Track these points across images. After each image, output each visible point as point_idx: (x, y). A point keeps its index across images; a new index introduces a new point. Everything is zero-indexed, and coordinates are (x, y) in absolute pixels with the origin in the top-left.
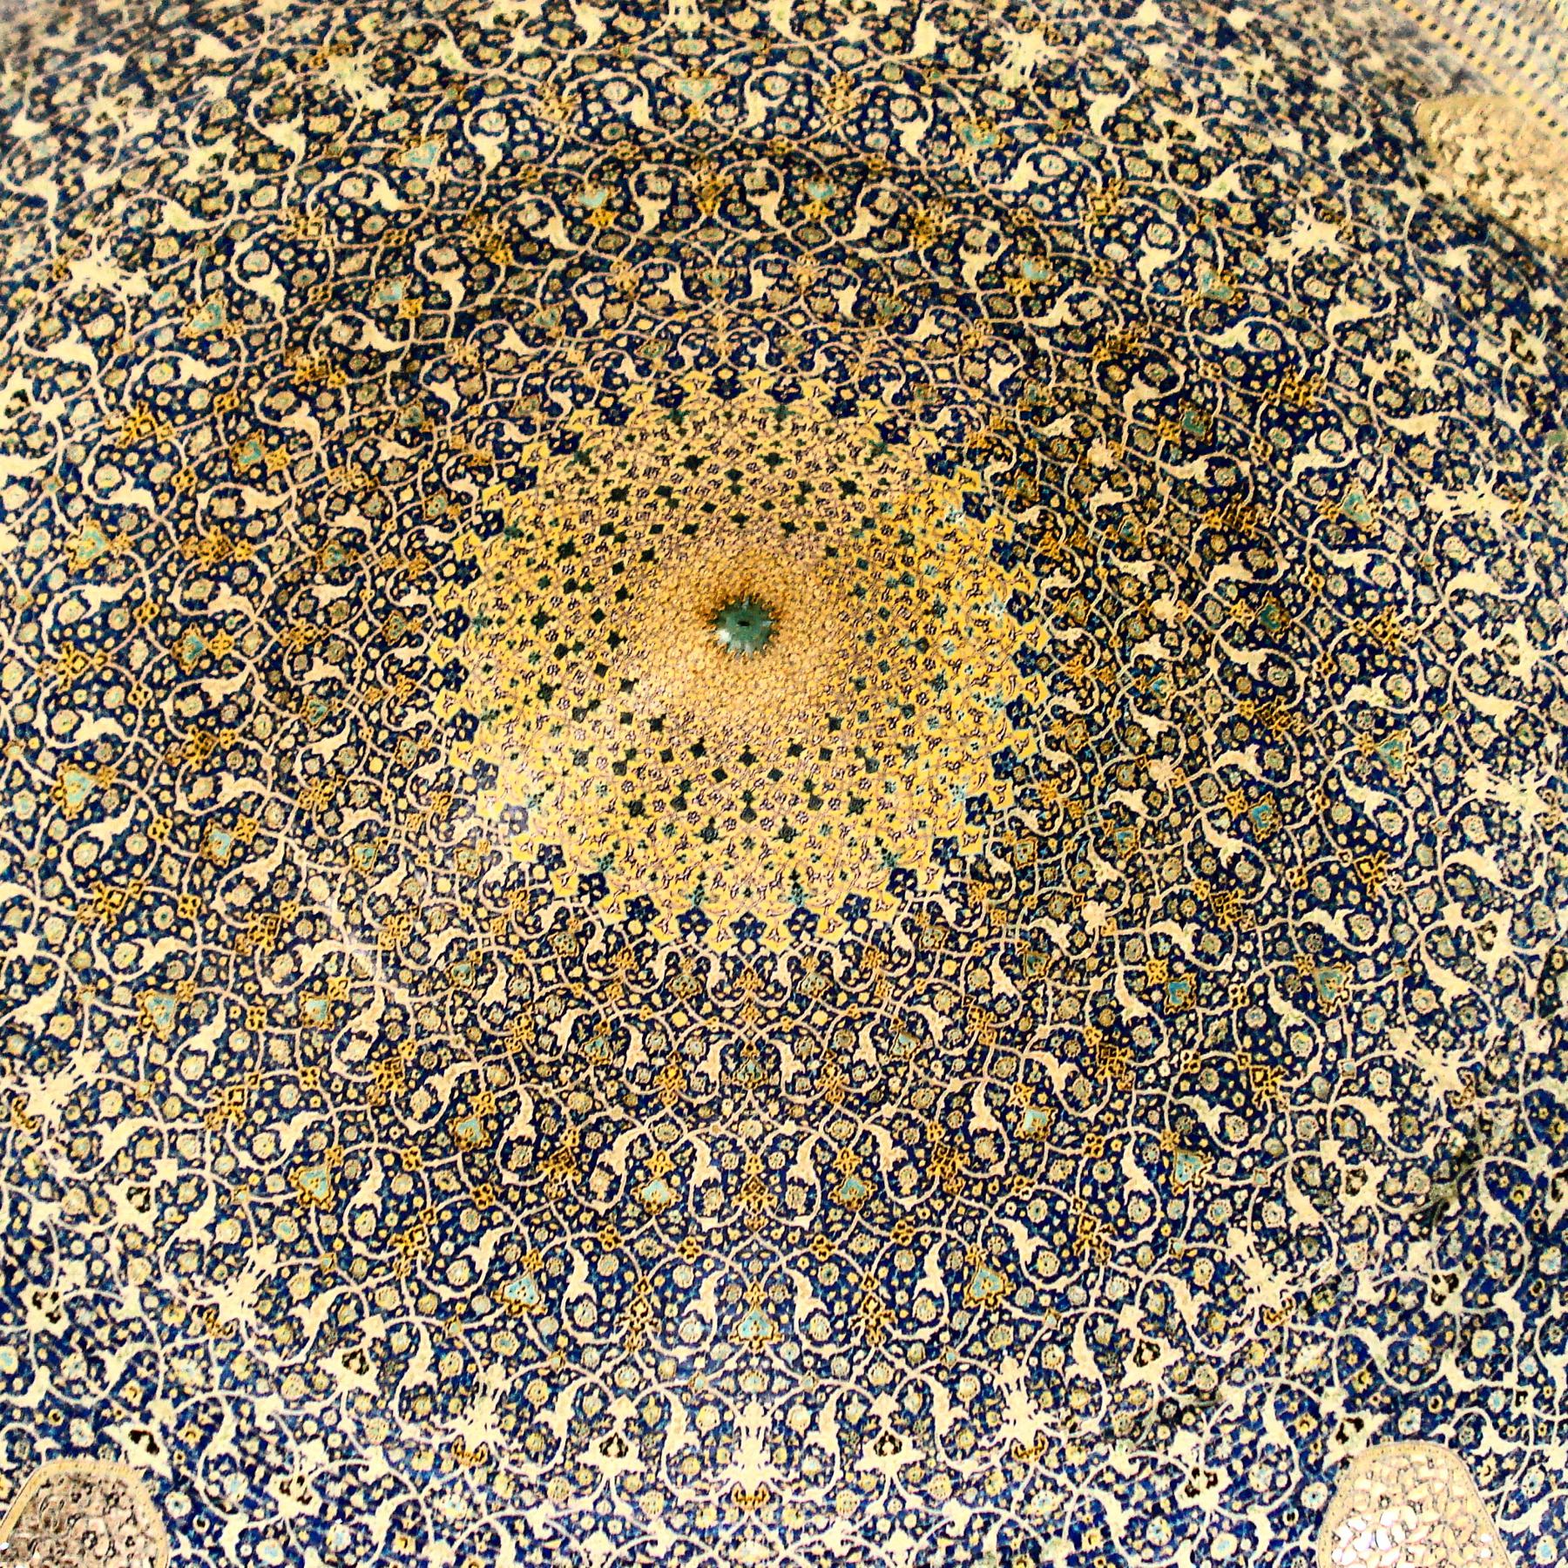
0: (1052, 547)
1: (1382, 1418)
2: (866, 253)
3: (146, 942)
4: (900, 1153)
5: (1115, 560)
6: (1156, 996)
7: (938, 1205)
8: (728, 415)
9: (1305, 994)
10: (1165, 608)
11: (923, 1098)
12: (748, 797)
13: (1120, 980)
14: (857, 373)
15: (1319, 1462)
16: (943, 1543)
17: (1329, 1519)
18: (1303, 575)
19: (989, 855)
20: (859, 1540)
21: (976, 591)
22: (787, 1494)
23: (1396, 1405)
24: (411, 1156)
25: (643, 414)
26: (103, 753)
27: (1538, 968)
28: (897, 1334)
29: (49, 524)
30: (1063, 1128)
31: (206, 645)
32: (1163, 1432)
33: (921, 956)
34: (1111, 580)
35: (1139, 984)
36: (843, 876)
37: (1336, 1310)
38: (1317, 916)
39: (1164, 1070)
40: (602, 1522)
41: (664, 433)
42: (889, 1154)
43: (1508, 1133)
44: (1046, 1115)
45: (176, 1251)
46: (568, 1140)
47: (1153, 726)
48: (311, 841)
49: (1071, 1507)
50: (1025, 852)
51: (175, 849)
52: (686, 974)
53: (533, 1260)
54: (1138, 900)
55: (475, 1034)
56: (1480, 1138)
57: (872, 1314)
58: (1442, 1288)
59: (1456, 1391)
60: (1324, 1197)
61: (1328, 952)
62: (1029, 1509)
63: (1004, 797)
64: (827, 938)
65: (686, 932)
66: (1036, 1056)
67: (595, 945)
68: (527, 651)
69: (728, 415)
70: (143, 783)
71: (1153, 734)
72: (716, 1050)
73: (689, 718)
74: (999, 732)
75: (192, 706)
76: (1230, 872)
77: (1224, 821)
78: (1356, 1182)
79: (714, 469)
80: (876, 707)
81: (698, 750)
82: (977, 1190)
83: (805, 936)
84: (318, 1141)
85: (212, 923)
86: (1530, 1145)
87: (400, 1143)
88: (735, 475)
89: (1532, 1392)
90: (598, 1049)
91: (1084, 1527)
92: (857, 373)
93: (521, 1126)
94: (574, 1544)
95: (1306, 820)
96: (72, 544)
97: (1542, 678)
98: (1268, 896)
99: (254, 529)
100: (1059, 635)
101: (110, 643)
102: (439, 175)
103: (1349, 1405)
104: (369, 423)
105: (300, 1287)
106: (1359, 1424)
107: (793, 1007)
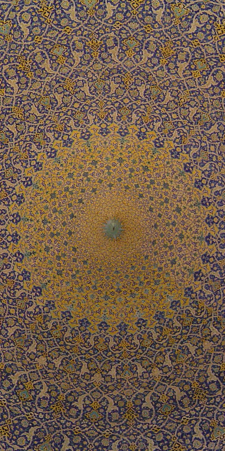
0: (167, 331)
5: (168, 353)
6: (21, 387)
8: (199, 221)
9: (38, 440)
10: (156, 372)
12: (58, 234)
18: (186, 418)
19: (53, 321)
21: (143, 307)
25: (198, 193)
26: (100, 12)
34: (161, 353)
35: (23, 380)
36: (36, 270)
38: (67, 440)
41: (191, 200)
47: (113, 372)
48: (54, 82)
50: (56, 333)
51: (60, 35)
54: (51, 375)
63: (73, 324)
64: (15, 266)
68: (137, 160)
69: (199, 221)
70: (86, 25)
71: (109, 373)
73: (83, 212)
74: (95, 321)
75: (110, 43)
76: (71, 407)
77: (88, 402)
81: (72, 216)
83: (15, 258)
85: (31, 48)
88: (174, 224)
95: (98, 430)
96: (181, 6)
98: (67, 421)
99: (171, 66)
100: (135, 337)
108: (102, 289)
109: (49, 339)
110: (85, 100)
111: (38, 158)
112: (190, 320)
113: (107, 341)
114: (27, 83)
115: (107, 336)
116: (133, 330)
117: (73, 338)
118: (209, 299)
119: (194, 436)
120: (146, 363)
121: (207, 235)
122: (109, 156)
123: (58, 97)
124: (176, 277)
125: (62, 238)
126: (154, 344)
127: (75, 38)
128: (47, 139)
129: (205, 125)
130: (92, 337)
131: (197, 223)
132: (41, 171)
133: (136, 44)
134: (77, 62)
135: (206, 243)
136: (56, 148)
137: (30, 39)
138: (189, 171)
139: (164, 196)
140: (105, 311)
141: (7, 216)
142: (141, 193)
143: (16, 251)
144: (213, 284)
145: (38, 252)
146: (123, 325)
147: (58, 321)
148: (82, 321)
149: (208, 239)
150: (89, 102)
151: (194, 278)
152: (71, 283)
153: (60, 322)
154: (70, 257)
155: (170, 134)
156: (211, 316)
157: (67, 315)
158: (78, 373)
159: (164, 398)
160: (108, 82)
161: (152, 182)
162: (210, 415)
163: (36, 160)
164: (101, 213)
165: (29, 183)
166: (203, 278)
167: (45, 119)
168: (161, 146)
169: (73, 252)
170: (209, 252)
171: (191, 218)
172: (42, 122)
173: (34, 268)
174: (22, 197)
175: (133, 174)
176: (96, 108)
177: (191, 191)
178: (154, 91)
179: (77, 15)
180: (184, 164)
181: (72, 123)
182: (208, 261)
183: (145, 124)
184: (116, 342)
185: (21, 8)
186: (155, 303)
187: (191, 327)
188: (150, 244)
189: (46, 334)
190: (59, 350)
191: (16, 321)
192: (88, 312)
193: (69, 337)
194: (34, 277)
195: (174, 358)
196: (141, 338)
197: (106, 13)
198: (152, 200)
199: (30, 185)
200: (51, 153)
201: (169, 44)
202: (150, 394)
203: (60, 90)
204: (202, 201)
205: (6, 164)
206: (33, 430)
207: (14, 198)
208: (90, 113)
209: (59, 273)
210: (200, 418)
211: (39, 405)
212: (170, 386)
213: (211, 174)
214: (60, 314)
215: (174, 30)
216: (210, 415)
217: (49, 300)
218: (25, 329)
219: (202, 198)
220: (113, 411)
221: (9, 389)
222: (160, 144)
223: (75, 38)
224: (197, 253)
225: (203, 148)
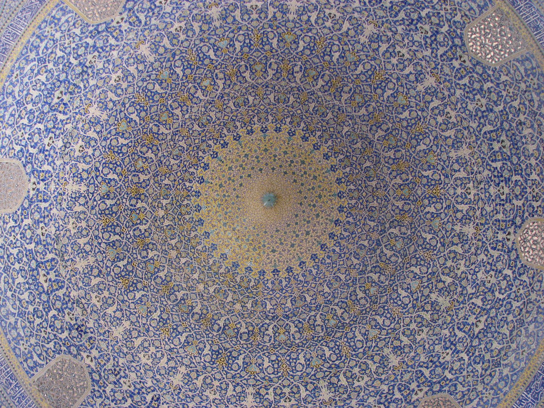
0: (229, 276)
1: (31, 196)
2: (313, 313)
3: (364, 71)
4: (160, 132)
5: (217, 286)
6: (138, 212)
7: (145, 130)
9: (114, 245)
10: (201, 287)
11: (164, 146)
12: (244, 169)
13: (146, 207)
14: (293, 281)
15: (33, 174)
16: (91, 74)
17: (22, 168)
18: (187, 323)
19: (189, 202)
20: (109, 58)
22: (132, 52)
23: (31, 202)
24: (269, 54)
26: (400, 110)
27: (86, 306)
28: (133, 100)
29: (444, 162)
30: (133, 169)
31: (389, 142)
32: (66, 141)
34: (214, 281)
35: (142, 210)
36: (213, 171)
37: (56, 200)
38: (125, 262)
39: (124, 200)
40: (171, 14)
42: (163, 130)
43: (61, 272)
44: (138, 167)
45: (316, 8)
46: (234, 79)
47: (183, 260)
48: (337, 107)
49: (71, 108)
52: (231, 127)
53: (225, 51)
54: (156, 224)
55: (270, 86)
56: (64, 264)
57: (141, 98)
58: (44, 231)
59: (25, 220)
60: (77, 215)
61: (118, 257)
62: (79, 98)
63: (195, 216)
66: (149, 176)
67: (256, 119)
69: (309, 250)
70: (386, 106)
71: (181, 259)
72: (214, 118)
73: (267, 175)
75: (384, 127)
76: (146, 250)
77: (156, 258)
78: (74, 225)
80: (232, 208)
82: (139, 141)
83: (212, 153)
84: (294, 46)
85: (350, 80)
86: (56, 276)
87: (274, 56)
88: (297, 236)
89: (14, 241)
90: (241, 100)
91: (65, 108)
92: (293, 281)
93: (247, 75)
94: (175, 5)
96: (435, 158)
97: (138, 359)
99: (394, 173)
100: (213, 259)
101: (413, 136)
102: (408, 281)
103: (38, 189)
104: (384, 209)
105: (279, 15)
106: (34, 189)
107: (204, 138)
110: (339, 133)
111: (284, 127)
113: (199, 243)
114: (326, 91)
119: (179, 336)
120: (202, 277)
122: (313, 169)
123: (330, 115)
125: (243, 173)
126: (217, 274)
127: (374, 104)
128: (299, 125)
129: (371, 217)
133: (394, 143)
134: (359, 114)
136: (297, 134)
137: (355, 76)
138: (336, 224)
143: (217, 150)
144: (277, 284)
148: (201, 220)
150: (339, 136)
155: (351, 198)
157: (198, 208)
158: (169, 239)
159: (189, 302)
160: (359, 140)
161: (314, 206)
162: (198, 337)
168: (340, 197)
172: (308, 115)
174: (252, 133)
178: (372, 173)
179: (388, 97)
181: (319, 133)
182: (288, 272)
185: (371, 60)
190: (174, 218)
191: (175, 180)
194: (208, 172)
195: (216, 291)
197: (401, 113)
201: (406, 164)
202: (186, 292)
203: (335, 114)
206: (117, 237)
209: (221, 186)
210: (193, 332)
211: (134, 230)
212: (199, 301)
214: (196, 203)
215: (417, 162)
216: (198, 337)
220: (161, 277)
221: (132, 205)
223: (374, 104)
225: (356, 224)
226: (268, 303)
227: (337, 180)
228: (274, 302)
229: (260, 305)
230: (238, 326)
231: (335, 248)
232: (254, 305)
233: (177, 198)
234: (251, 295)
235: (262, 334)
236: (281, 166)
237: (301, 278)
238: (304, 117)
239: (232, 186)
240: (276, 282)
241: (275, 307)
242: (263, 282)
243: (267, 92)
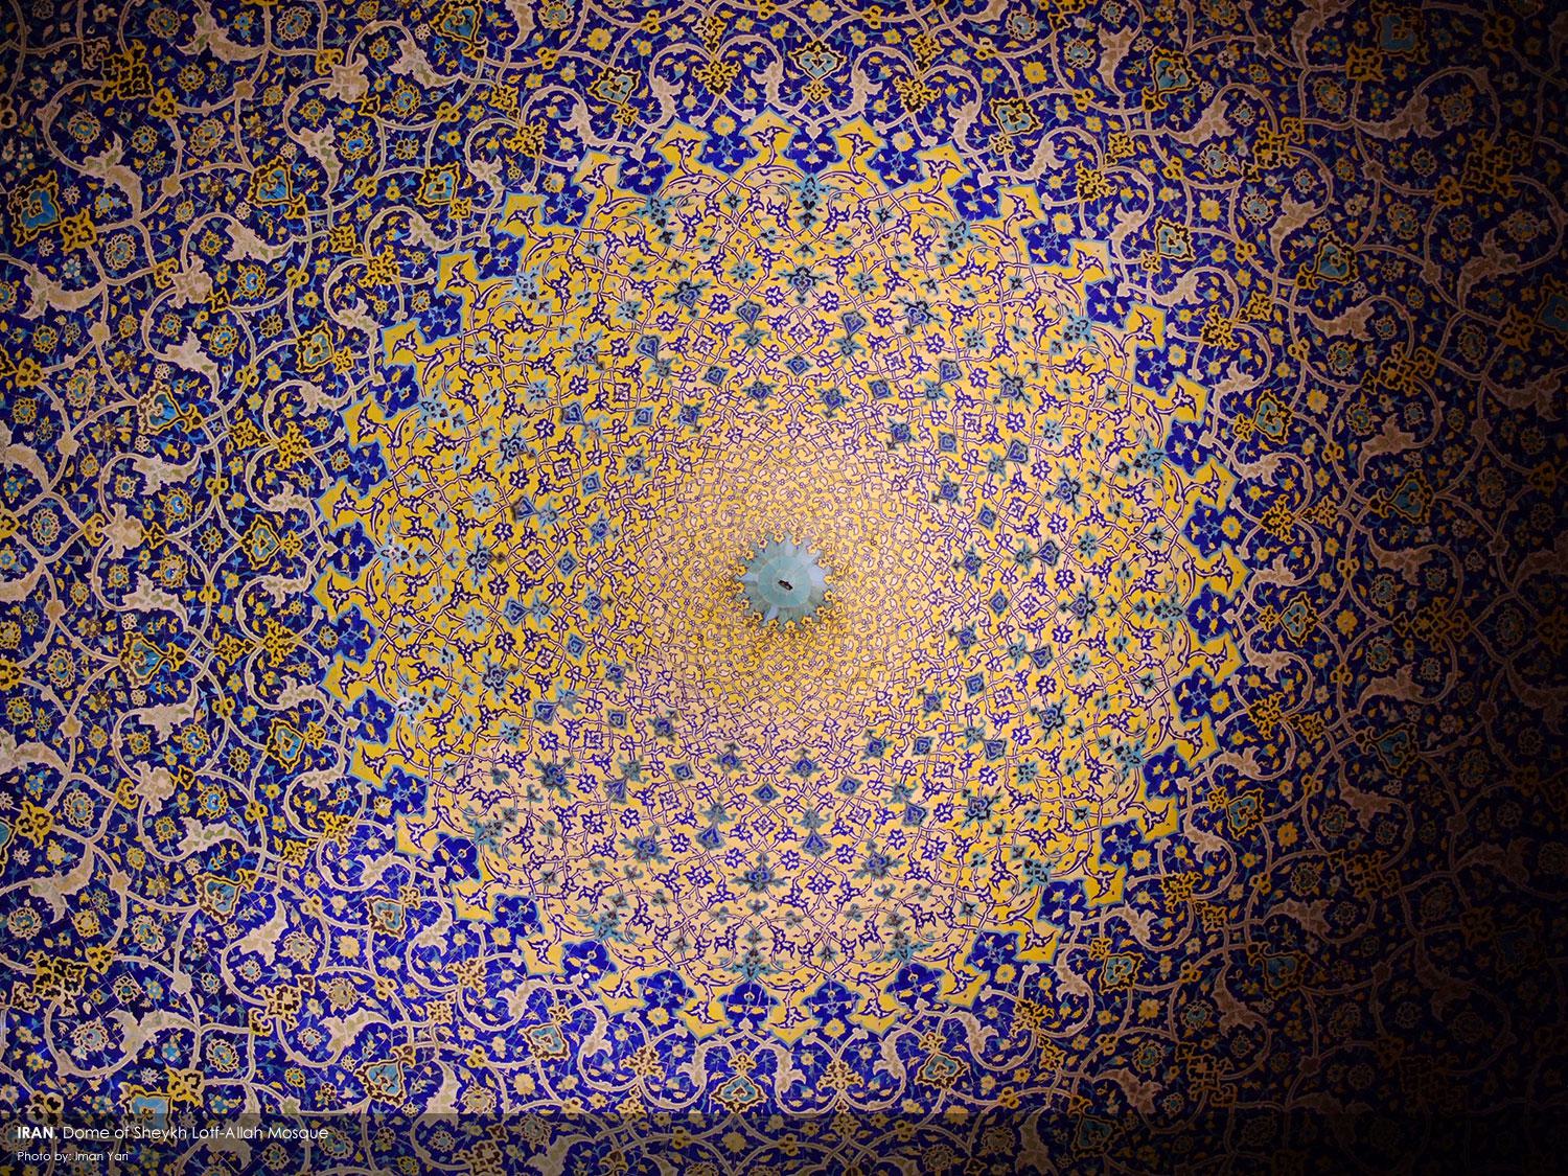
0: (278, 641)
5: (183, 614)
8: (681, 944)
10: (124, 534)
19: (497, 189)
33: (639, 63)
36: (733, 201)
41: (779, 944)
47: (189, 355)
54: (273, 96)
55: (1343, 168)
63: (455, 268)
65: (991, 191)
69: (681, 944)
71: (192, 341)
73: (900, 483)
76: (110, 127)
77: (104, 204)
79: (736, 857)
81: (900, 434)
83: (814, 132)
88: (710, 838)
98: (54, 86)
100: (304, 504)
107: (858, 38)
108: (552, 441)
109: (429, 144)
112: (288, 757)
113: (331, 381)
115: (353, 389)
116: (334, 507)
117: (397, 245)
118: (345, 865)
120: (177, 506)
121: (612, 958)
124: (487, 766)
125: (825, 360)
126: (245, 572)
130: (370, 327)
131: (674, 935)
132: (1130, 375)
135: (577, 941)
136: (1203, 474)
138: (902, 982)
139: (838, 841)
140: (457, 420)
141: (1001, 166)
142: (888, 752)
143: (844, 147)
144: (401, 904)
145: (806, 238)
146: (374, 471)
147: (488, 211)
148: (453, 312)
149: (592, 955)
151: (454, 835)
152: (628, 324)
153: (480, 218)
154: (736, 359)
156: (271, 848)
157: (500, 259)
158: (243, 211)
161: (914, 814)
163: (1184, 369)
164: (867, 557)
165: (1101, 309)
166: (440, 872)
167: (1340, 470)
168: (1048, 908)
169: (749, 383)
170: (538, 937)
171: (705, 917)
173: (744, 195)
174: (1053, 256)
175: (977, 748)
176: (1306, 698)
177: (816, 960)
180: (939, 973)
182: (501, 920)
183: (1164, 874)
184: (313, 417)
186: (412, 638)
187: (257, 746)
188: (663, 710)
189: (452, 139)
190: (367, 169)
191: (554, 41)
192: (481, 348)
193: (406, 232)
196: (289, 525)
198: (843, 787)
199: (1091, 307)
200: (1192, 445)
202: (40, 473)
204: (756, 989)
205: (1215, 240)
207: (1063, 224)
208: (1294, 665)
209: (686, 293)
213: (856, 1067)
214: (516, 230)
217: (591, 208)
218: (507, 64)
219: (770, 993)
222: (1055, 906)
224: (555, 889)
226: (278, 923)
227: (1123, 831)
228: (301, 949)
229: (234, 892)
230: (56, 854)
231: (784, 1059)
232: (217, 862)
233: (475, 113)
234: (257, 813)
235: (98, 996)
236: (987, 518)
237: (517, 1002)
238: (1309, 446)
239: (719, 355)
240: (410, 896)
241: (283, 972)
242: (363, 831)
243: (1302, 180)
